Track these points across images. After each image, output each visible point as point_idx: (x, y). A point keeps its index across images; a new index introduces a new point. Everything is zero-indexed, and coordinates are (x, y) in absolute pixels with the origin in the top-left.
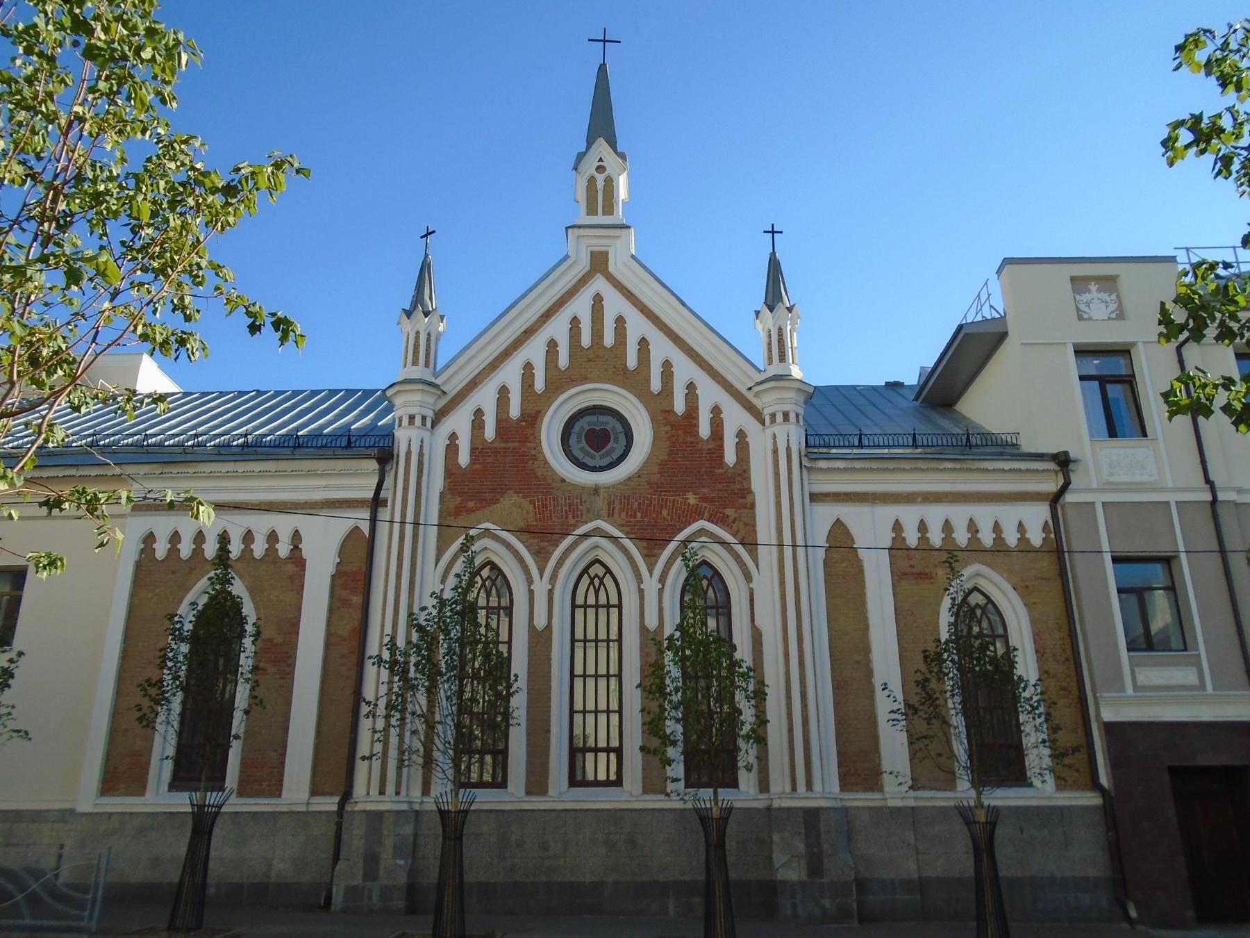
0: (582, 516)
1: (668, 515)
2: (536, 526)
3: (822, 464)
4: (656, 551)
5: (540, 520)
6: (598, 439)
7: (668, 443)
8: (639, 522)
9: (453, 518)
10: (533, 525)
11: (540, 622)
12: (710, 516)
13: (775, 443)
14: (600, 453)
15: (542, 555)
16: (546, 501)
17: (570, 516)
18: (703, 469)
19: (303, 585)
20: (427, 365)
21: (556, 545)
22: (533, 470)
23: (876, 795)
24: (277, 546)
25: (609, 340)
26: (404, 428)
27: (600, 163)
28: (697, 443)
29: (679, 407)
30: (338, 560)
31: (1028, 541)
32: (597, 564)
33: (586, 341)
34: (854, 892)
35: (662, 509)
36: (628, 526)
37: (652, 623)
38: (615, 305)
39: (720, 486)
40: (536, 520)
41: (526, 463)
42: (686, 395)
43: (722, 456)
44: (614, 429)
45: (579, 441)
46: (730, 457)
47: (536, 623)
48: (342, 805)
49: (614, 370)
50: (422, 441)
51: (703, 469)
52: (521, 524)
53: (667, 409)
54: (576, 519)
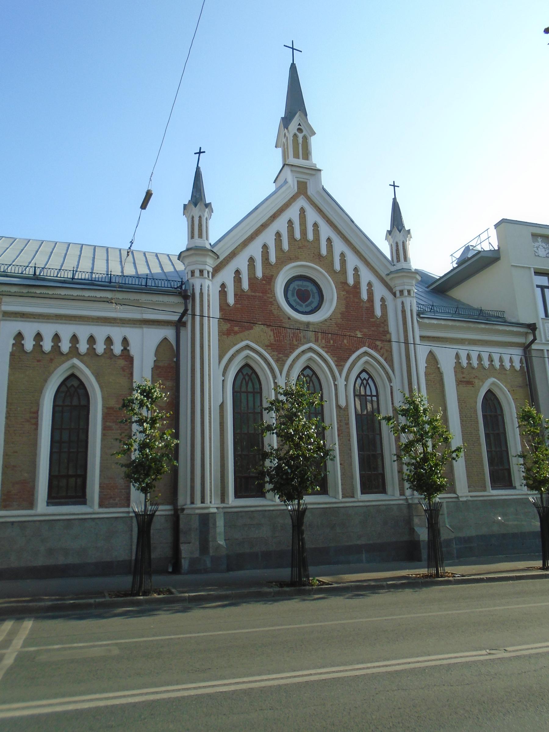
0: (301, 340)
1: (347, 343)
2: (276, 344)
4: (342, 363)
5: (278, 341)
6: (303, 296)
7: (345, 301)
9: (226, 336)
12: (369, 345)
13: (403, 307)
14: (305, 304)
15: (280, 362)
16: (280, 330)
17: (294, 340)
18: (364, 319)
21: (288, 356)
22: (271, 311)
23: (454, 495)
25: (310, 236)
27: (299, 127)
28: (360, 303)
29: (351, 281)
31: (514, 367)
32: (308, 369)
33: (298, 235)
36: (326, 348)
37: (343, 403)
38: (312, 216)
39: (373, 329)
40: (275, 341)
43: (374, 312)
44: (312, 290)
45: (293, 295)
46: (378, 312)
49: (314, 255)
52: (267, 343)
54: (298, 342)
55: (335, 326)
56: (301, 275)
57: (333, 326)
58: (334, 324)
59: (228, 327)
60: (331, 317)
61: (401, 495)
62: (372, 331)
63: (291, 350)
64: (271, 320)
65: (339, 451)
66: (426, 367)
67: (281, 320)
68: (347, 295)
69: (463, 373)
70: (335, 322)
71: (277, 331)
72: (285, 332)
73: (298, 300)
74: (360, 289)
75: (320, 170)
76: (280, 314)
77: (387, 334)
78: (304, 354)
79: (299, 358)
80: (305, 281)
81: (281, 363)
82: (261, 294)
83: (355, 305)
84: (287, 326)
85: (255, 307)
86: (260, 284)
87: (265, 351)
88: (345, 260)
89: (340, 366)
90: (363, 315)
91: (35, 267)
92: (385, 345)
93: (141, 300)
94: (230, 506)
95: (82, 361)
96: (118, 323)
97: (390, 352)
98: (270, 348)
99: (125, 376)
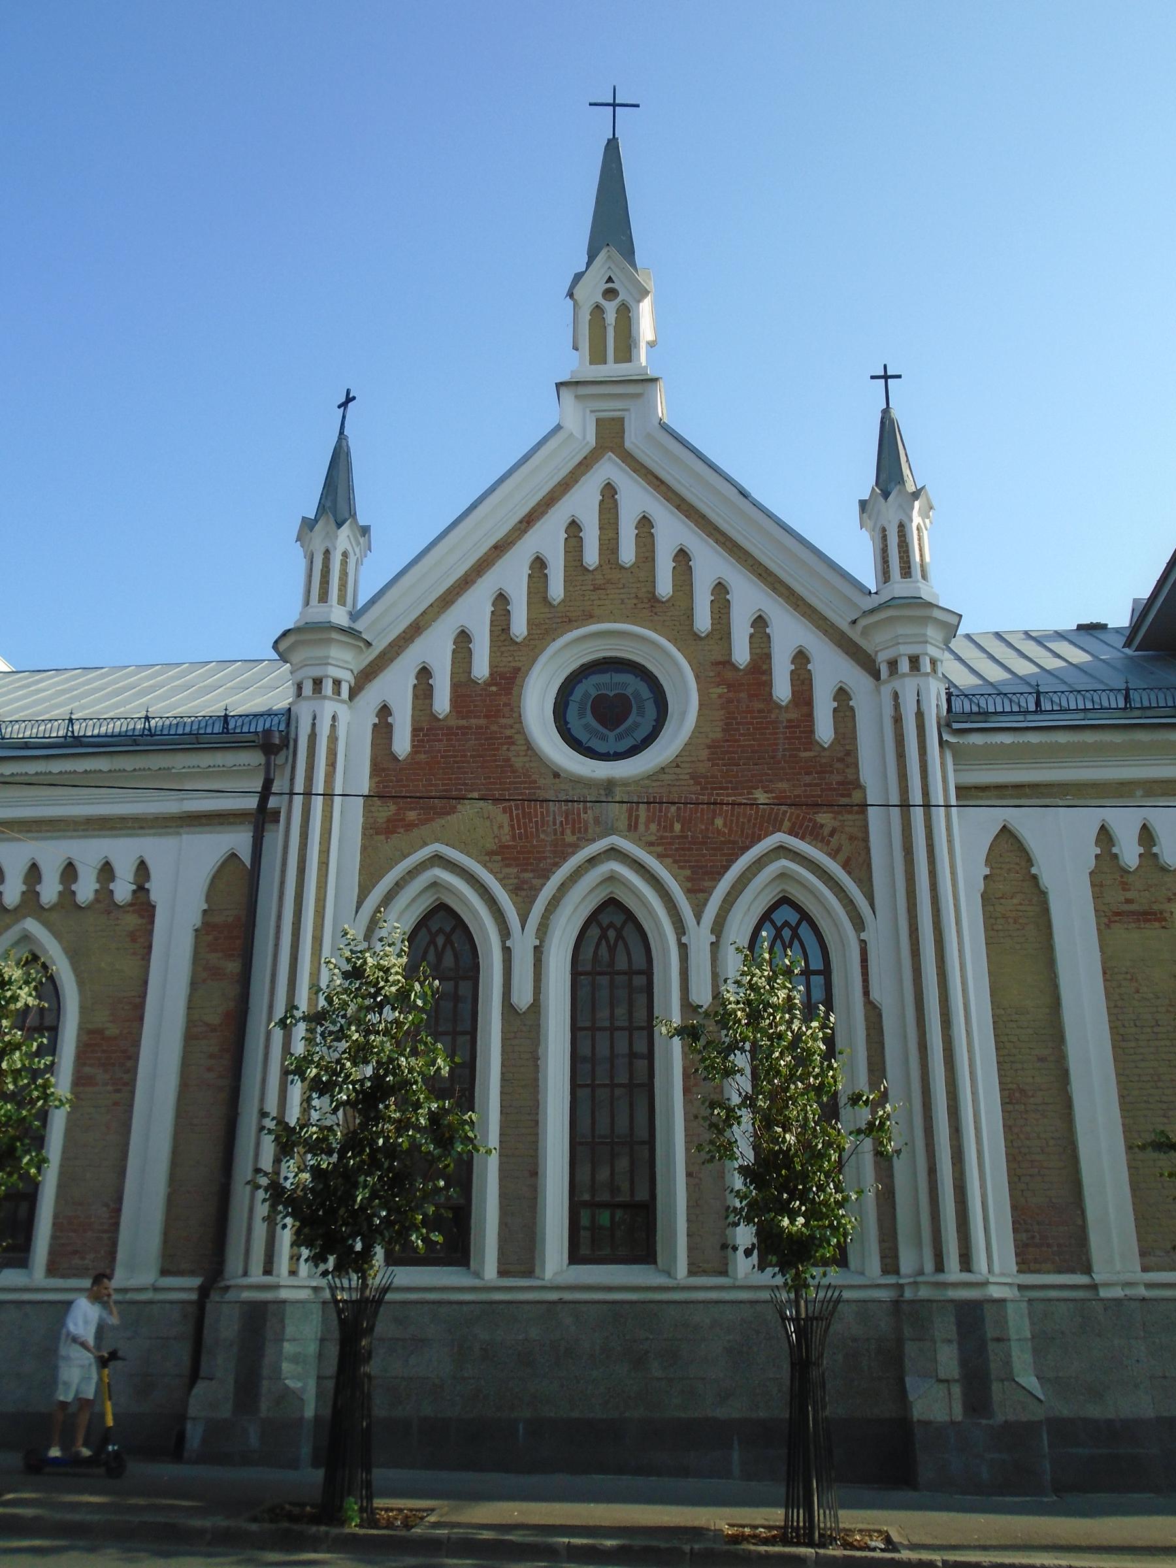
1: (725, 825)
2: (515, 847)
3: (977, 739)
4: (707, 884)
5: (520, 838)
7: (722, 712)
8: (678, 837)
9: (382, 837)
10: (508, 847)
11: (523, 998)
12: (794, 825)
13: (897, 706)
15: (523, 893)
17: (568, 832)
18: (780, 754)
19: (150, 947)
20: (342, 601)
21: (546, 876)
22: (508, 760)
23: (1081, 1279)
24: (112, 886)
25: (628, 554)
26: (308, 698)
27: (610, 285)
28: (770, 711)
29: (742, 655)
30: (205, 907)
33: (591, 557)
34: (1046, 1442)
35: (714, 818)
36: (658, 845)
39: (807, 779)
40: (514, 838)
41: (497, 750)
42: (751, 636)
43: (812, 732)
44: (637, 694)
45: (582, 714)
46: (825, 730)
47: (515, 1000)
48: (204, 1292)
49: (635, 601)
50: (334, 718)
51: (780, 754)
52: (490, 845)
53: (720, 659)
54: (578, 835)
55: (692, 782)
56: (604, 658)
57: (682, 783)
58: (687, 777)
59: (390, 813)
60: (679, 759)
61: (885, 1271)
62: (805, 785)
63: (557, 860)
64: (505, 783)
66: (986, 877)
67: (535, 782)
68: (731, 695)
69: (1125, 887)
70: (690, 771)
71: (520, 812)
72: (542, 813)
73: (594, 723)
74: (771, 674)
75: (654, 380)
76: (532, 765)
77: (854, 789)
78: (594, 866)
79: (580, 878)
80: (618, 671)
81: (527, 896)
82: (482, 722)
83: (752, 718)
84: (550, 795)
85: (465, 756)
86: (481, 695)
87: (485, 866)
88: (728, 601)
89: (698, 891)
90: (777, 745)
91: (71, 720)
92: (846, 823)
93: (173, 768)
95: (47, 924)
96: (134, 828)
97: (863, 839)
98: (499, 858)
99: (134, 954)
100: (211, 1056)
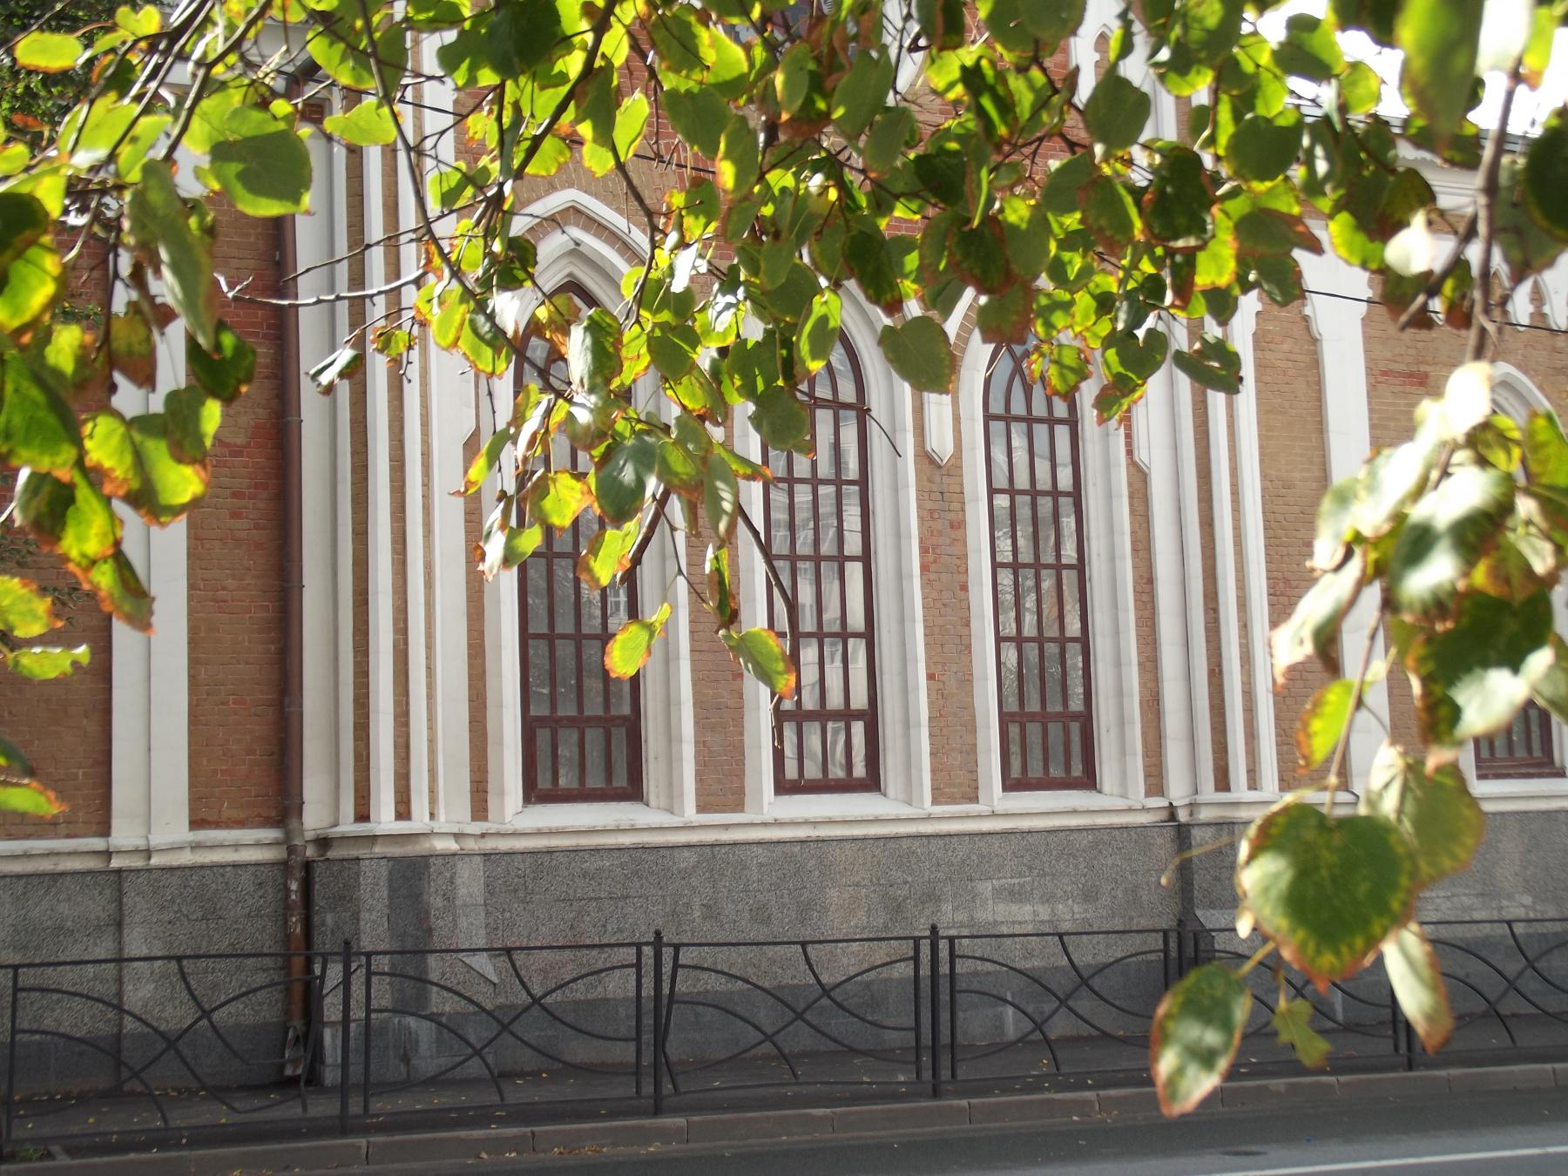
61: (1148, 794)
65: (926, 627)
66: (1258, 313)
94: (509, 828)
100: (235, 495)
